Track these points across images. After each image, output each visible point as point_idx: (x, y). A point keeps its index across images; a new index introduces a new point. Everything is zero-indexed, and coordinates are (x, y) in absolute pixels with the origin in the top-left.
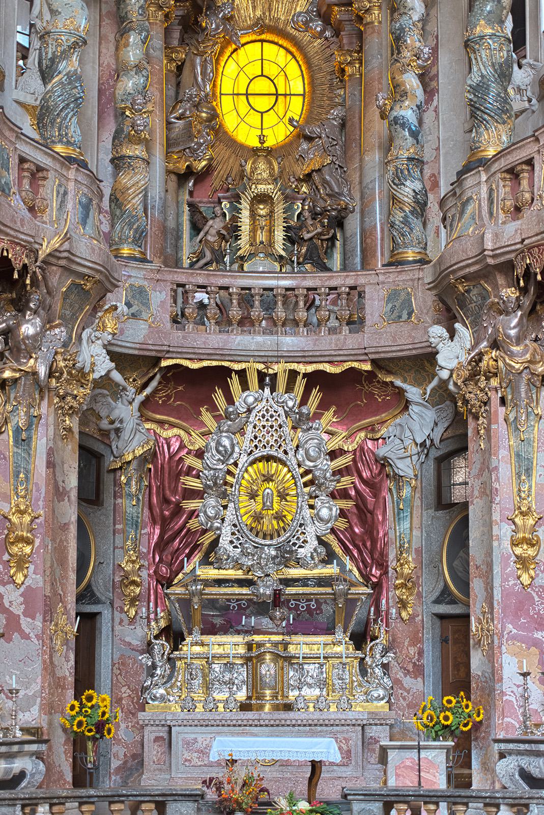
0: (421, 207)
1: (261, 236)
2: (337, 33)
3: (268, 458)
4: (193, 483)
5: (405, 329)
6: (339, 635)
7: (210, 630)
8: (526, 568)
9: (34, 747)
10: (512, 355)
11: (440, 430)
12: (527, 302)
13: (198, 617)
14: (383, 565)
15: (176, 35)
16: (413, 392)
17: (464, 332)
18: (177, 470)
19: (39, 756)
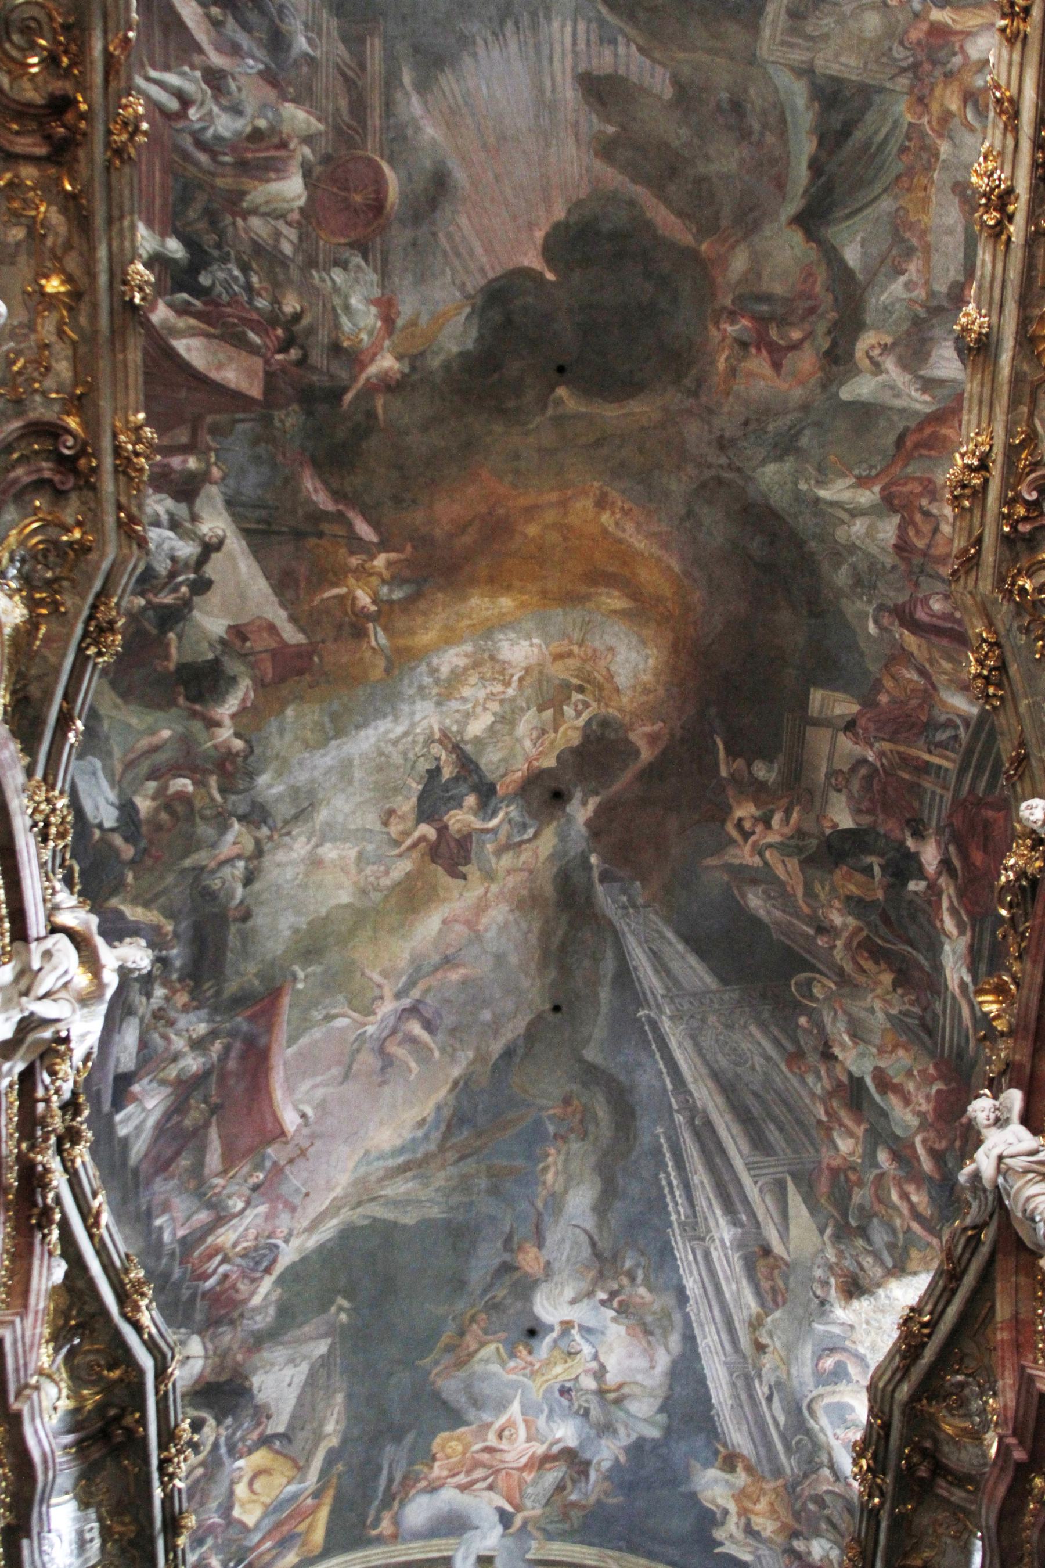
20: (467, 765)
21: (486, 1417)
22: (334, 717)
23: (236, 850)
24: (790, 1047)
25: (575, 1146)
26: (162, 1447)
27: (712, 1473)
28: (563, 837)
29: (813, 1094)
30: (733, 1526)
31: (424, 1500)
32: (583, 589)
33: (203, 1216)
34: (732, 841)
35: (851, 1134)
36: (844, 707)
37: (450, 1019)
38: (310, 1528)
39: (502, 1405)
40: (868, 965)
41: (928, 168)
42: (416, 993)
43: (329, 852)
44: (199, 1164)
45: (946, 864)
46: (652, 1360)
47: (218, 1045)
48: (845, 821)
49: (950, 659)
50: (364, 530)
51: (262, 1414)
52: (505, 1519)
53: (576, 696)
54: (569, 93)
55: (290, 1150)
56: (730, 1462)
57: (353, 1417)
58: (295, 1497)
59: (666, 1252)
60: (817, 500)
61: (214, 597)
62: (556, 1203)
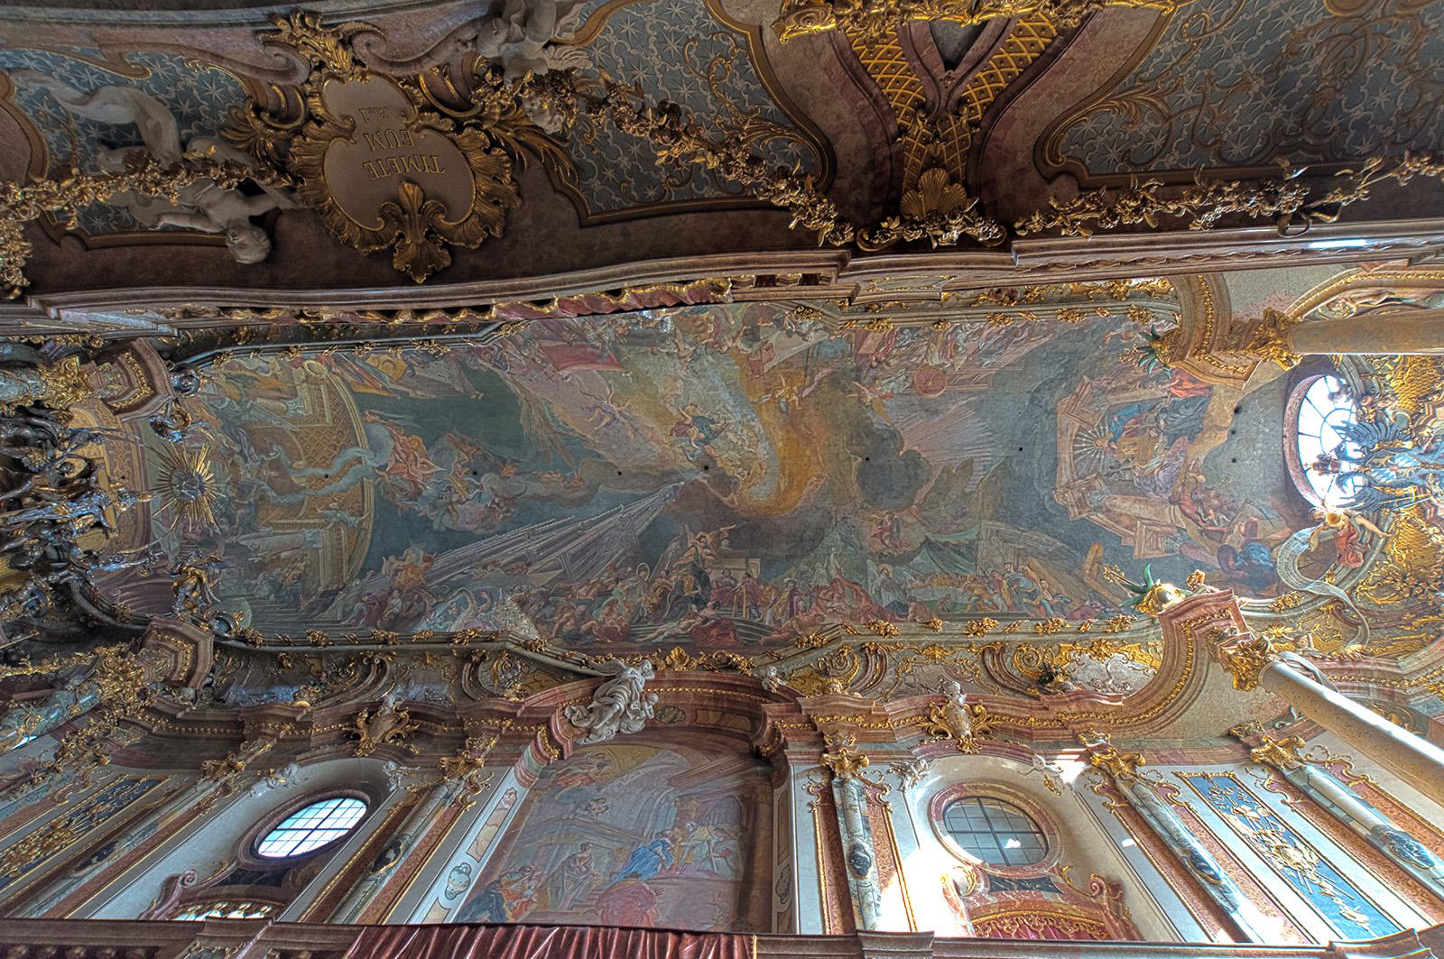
20: (717, 434)
22: (735, 384)
23: (682, 349)
24: (617, 565)
25: (562, 485)
27: (422, 553)
28: (690, 471)
29: (600, 576)
31: (387, 433)
32: (786, 472)
33: (521, 340)
34: (696, 535)
35: (587, 594)
36: (755, 573)
37: (611, 433)
40: (658, 592)
41: (952, 584)
42: (622, 419)
43: (680, 384)
44: (545, 338)
45: (707, 620)
46: (470, 523)
47: (598, 344)
48: (712, 578)
49: (783, 611)
50: (807, 391)
51: (424, 365)
52: (382, 468)
53: (746, 473)
54: (967, 456)
55: (551, 373)
59: (522, 524)
60: (829, 555)
61: (784, 338)
62: (537, 479)
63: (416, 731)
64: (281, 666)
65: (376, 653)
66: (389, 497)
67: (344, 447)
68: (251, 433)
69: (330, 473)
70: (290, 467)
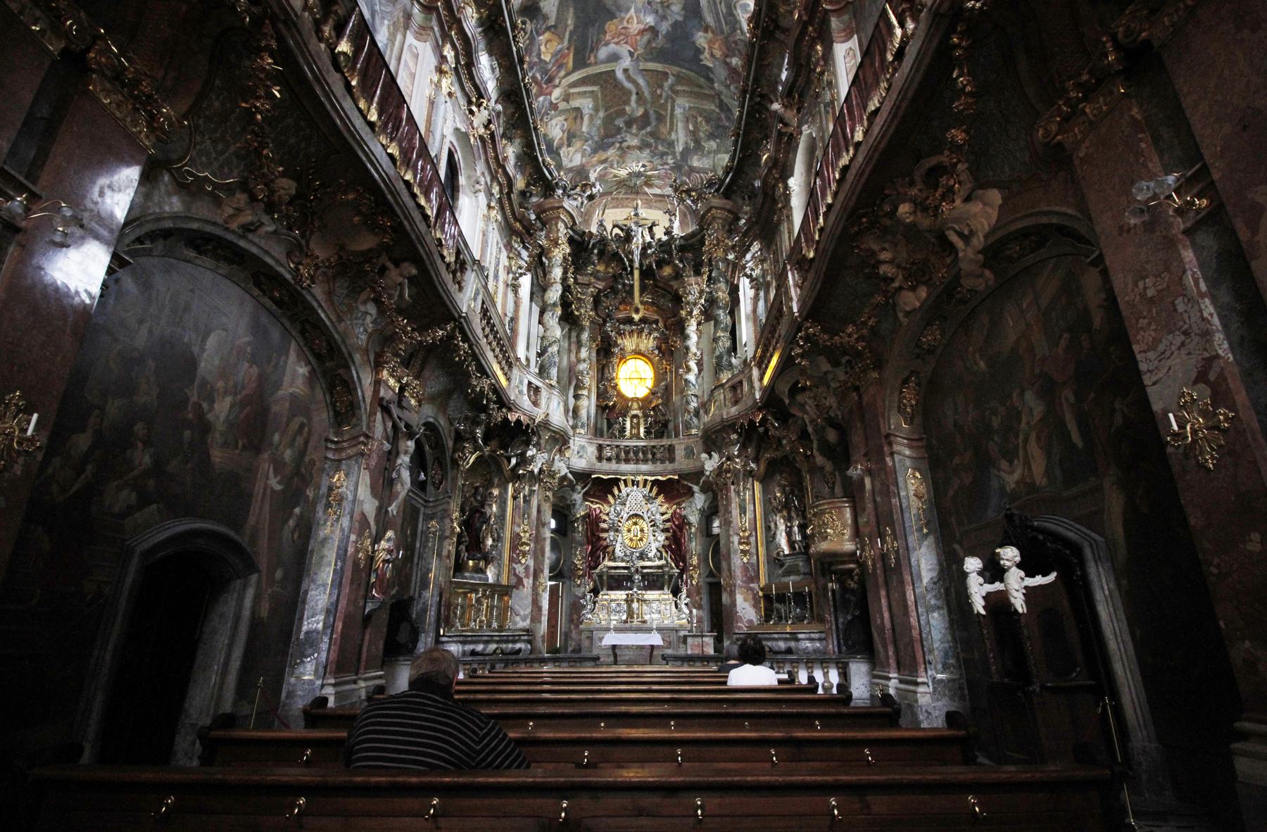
0: (697, 414)
1: (634, 431)
2: (664, 355)
3: (636, 515)
4: (604, 526)
5: (692, 461)
6: (666, 591)
7: (611, 588)
8: (745, 556)
9: (526, 638)
10: (736, 463)
11: (707, 504)
12: (741, 440)
13: (605, 583)
14: (684, 561)
15: (602, 354)
16: (696, 488)
17: (715, 456)
18: (598, 519)
19: (529, 642)
21: (623, 15)
26: (513, 31)
27: (701, 34)
30: (706, 54)
31: (604, 48)
38: (567, 63)
39: (628, 10)
51: (545, 18)
52: (631, 54)
56: (706, 29)
57: (577, 16)
58: (561, 50)
63: (799, 96)
64: (750, 156)
65: (751, 99)
66: (655, 54)
67: (615, 79)
68: (607, 136)
69: (634, 90)
70: (630, 116)
